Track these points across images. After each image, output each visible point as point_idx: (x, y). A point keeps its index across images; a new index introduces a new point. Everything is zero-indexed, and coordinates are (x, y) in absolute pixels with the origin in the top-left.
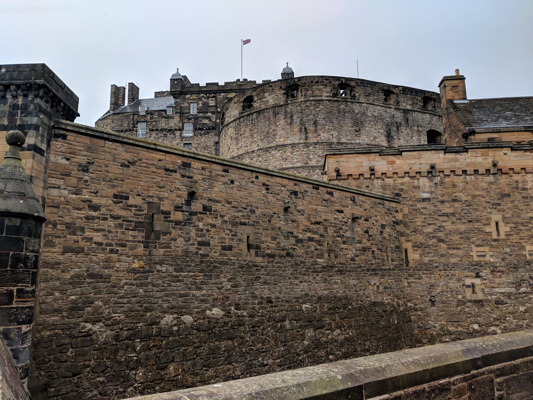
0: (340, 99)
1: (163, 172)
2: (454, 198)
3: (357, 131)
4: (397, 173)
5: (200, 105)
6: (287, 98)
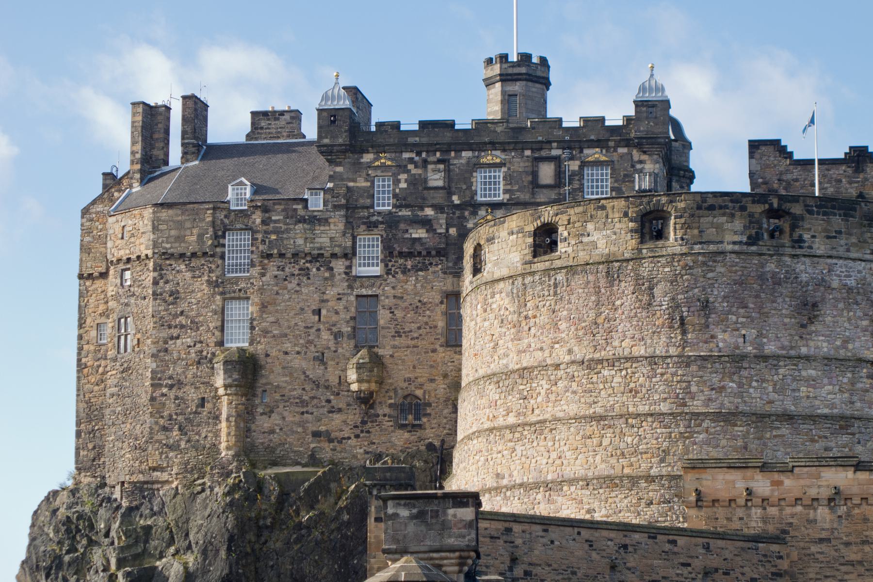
0: (764, 250)
1: (488, 540)
2: (864, 539)
3: (803, 326)
4: (784, 499)
5: (403, 185)
6: (642, 242)
